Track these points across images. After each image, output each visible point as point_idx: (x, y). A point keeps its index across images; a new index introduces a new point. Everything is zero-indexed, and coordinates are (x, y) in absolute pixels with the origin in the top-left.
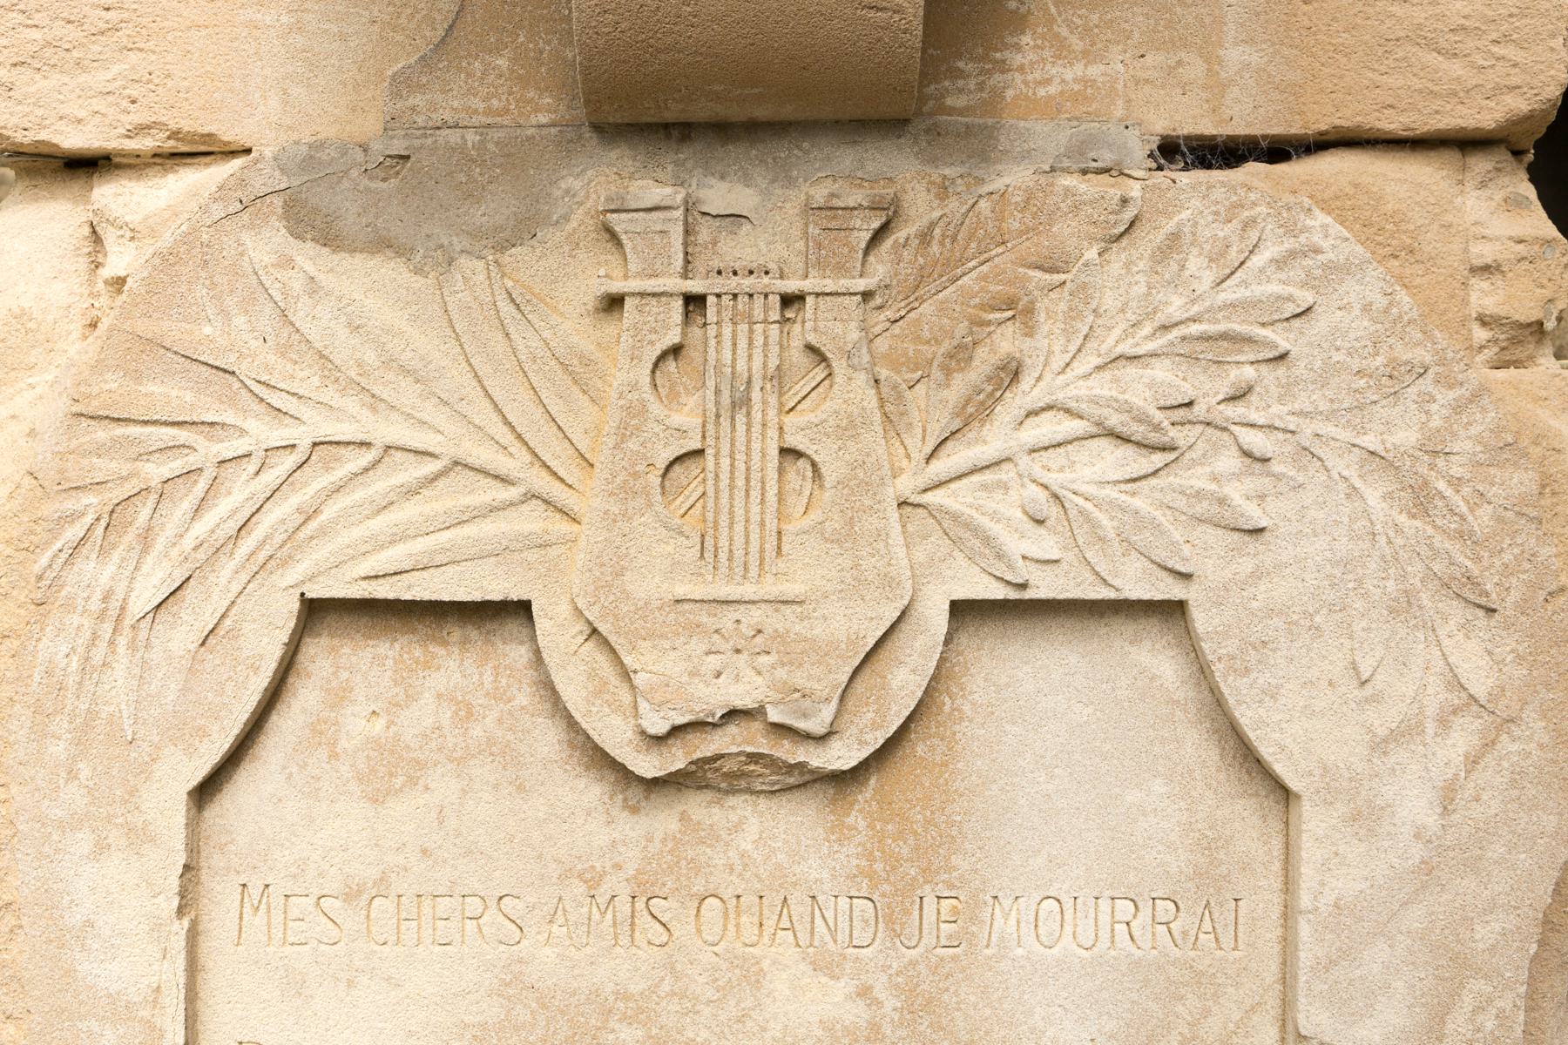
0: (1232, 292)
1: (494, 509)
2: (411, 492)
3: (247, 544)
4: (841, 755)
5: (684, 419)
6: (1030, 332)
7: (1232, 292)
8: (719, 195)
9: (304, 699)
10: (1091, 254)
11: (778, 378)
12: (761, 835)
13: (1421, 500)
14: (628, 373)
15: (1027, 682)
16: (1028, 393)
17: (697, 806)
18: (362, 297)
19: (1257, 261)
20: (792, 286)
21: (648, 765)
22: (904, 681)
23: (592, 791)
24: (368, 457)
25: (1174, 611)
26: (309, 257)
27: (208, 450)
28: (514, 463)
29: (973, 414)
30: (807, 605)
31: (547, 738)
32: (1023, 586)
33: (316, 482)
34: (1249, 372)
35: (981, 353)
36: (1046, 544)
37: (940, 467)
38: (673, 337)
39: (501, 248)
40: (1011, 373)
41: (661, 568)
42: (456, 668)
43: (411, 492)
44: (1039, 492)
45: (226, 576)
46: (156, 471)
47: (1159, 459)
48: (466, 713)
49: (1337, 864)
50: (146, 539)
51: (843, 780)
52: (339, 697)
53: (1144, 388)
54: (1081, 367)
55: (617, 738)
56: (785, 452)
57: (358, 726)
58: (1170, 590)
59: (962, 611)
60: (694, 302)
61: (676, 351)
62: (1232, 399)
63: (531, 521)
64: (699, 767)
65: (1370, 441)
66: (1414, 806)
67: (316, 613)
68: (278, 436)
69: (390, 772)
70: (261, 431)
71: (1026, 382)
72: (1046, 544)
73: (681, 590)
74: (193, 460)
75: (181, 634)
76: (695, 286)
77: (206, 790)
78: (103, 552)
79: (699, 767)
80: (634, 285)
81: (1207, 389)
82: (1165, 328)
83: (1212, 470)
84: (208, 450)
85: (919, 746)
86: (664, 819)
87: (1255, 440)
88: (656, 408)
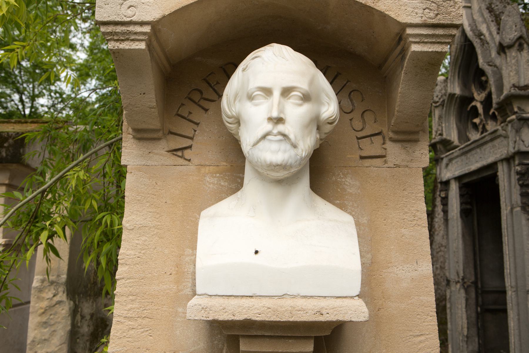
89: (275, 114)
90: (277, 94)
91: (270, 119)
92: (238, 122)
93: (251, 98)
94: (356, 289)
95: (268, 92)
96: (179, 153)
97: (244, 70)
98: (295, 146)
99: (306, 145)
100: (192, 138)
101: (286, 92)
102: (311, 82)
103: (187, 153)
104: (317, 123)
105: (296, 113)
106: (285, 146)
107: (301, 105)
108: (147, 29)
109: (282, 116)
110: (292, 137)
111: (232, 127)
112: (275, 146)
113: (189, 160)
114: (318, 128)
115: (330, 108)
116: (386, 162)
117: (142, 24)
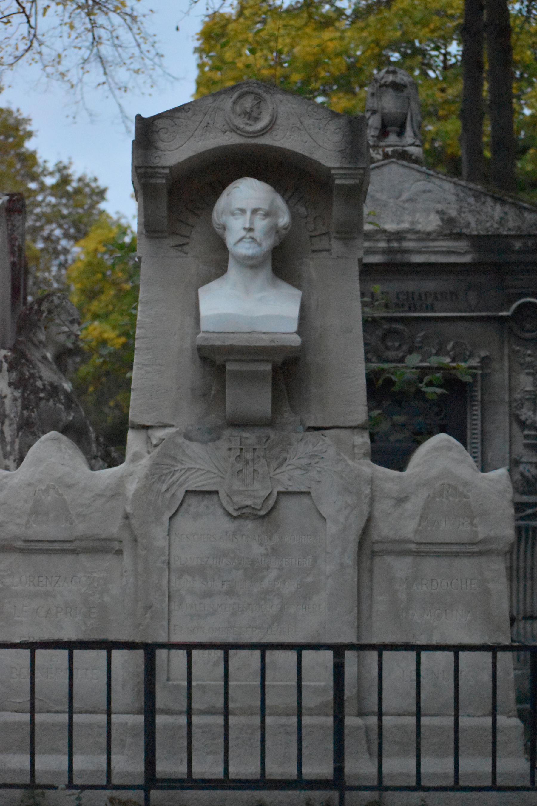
0: (315, 449)
1: (213, 478)
2: (202, 475)
3: (178, 483)
4: (263, 513)
5: (239, 466)
6: (288, 453)
7: (315, 449)
8: (244, 435)
9: (185, 505)
10: (296, 443)
11: (253, 460)
12: (249, 525)
13: (342, 477)
14: (233, 459)
15: (287, 503)
16: (288, 462)
17: (242, 522)
18: (195, 448)
19: (319, 444)
20: (255, 447)
21: (235, 514)
22: (271, 502)
23: (226, 519)
24: (195, 470)
25: (309, 493)
26: (187, 442)
27: (173, 469)
28: (216, 471)
29: (280, 465)
30: (258, 492)
31: (220, 511)
32: (287, 489)
33: (189, 473)
34: (318, 460)
35: (281, 457)
36: (290, 483)
37: (276, 472)
38: (238, 454)
39: (214, 441)
40: (285, 459)
41: (237, 485)
42: (206, 501)
43: (202, 475)
44: (289, 477)
45: (175, 486)
46: (165, 472)
47: (305, 472)
48: (208, 507)
49: (332, 529)
50: (163, 482)
51: (263, 517)
52: (189, 506)
53: (304, 462)
54: (295, 459)
55: (230, 510)
56: (254, 470)
57: (192, 510)
58: (308, 490)
59: (279, 493)
60: (241, 449)
61: (239, 456)
62: (316, 463)
63: (219, 479)
64: (243, 514)
65: (335, 469)
66: (342, 520)
67: (187, 492)
68: (183, 467)
69: (196, 516)
70: (180, 467)
71: (288, 460)
72: (290, 483)
73: (240, 489)
74: (170, 470)
75: (168, 495)
76: (241, 447)
77: (171, 518)
78: (158, 483)
79: (243, 514)
80: (233, 447)
81: (313, 462)
82: (306, 453)
83: (313, 473)
84: (173, 469)
85: (274, 514)
86: (237, 523)
87: (318, 469)
88: (236, 464)
89: (247, 226)
90: (249, 213)
91: (245, 229)
92: (224, 228)
93: (233, 214)
94: (294, 327)
95: (243, 211)
96: (180, 248)
97: (228, 195)
98: (260, 245)
99: (267, 244)
100: (188, 237)
101: (255, 211)
102: (272, 203)
103: (186, 248)
104: (275, 229)
105: (261, 224)
106: (254, 245)
107: (264, 219)
108: (167, 171)
109: (252, 227)
110: (258, 239)
111: (219, 231)
112: (247, 245)
113: (186, 253)
114: (277, 232)
115: (284, 220)
116: (331, 254)
117: (164, 168)
